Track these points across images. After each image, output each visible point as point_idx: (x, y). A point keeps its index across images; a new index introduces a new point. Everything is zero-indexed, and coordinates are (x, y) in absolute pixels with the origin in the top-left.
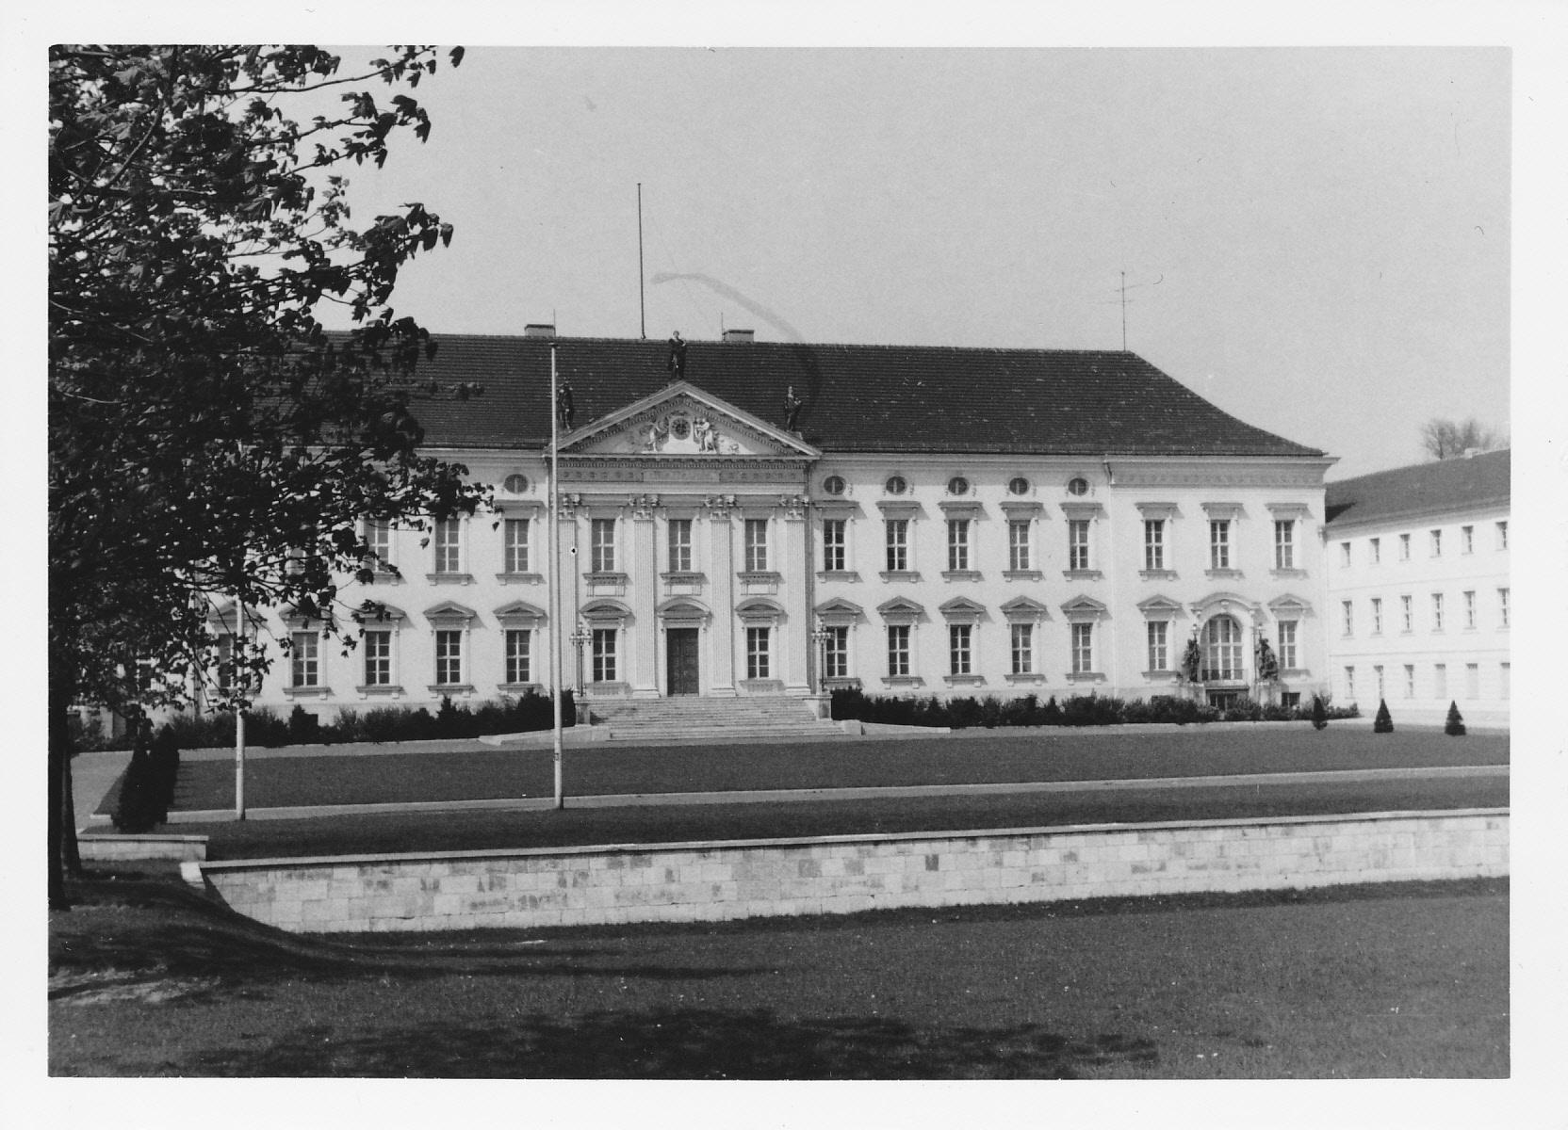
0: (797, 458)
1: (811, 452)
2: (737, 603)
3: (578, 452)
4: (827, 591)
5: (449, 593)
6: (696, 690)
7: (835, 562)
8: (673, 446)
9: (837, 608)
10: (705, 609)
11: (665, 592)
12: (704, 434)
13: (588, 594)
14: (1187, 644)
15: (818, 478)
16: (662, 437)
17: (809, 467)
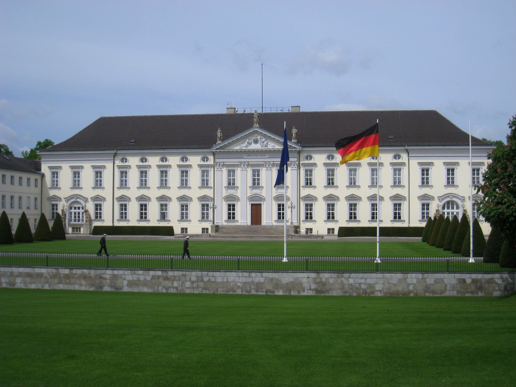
0: (293, 149)
1: (298, 148)
2: (273, 196)
3: (222, 149)
4: (305, 192)
5: (184, 192)
6: (261, 224)
7: (309, 183)
8: (254, 147)
9: (308, 197)
10: (263, 197)
11: (250, 193)
12: (264, 142)
13: (225, 193)
14: (436, 211)
15: (303, 155)
16: (250, 144)
17: (299, 152)
